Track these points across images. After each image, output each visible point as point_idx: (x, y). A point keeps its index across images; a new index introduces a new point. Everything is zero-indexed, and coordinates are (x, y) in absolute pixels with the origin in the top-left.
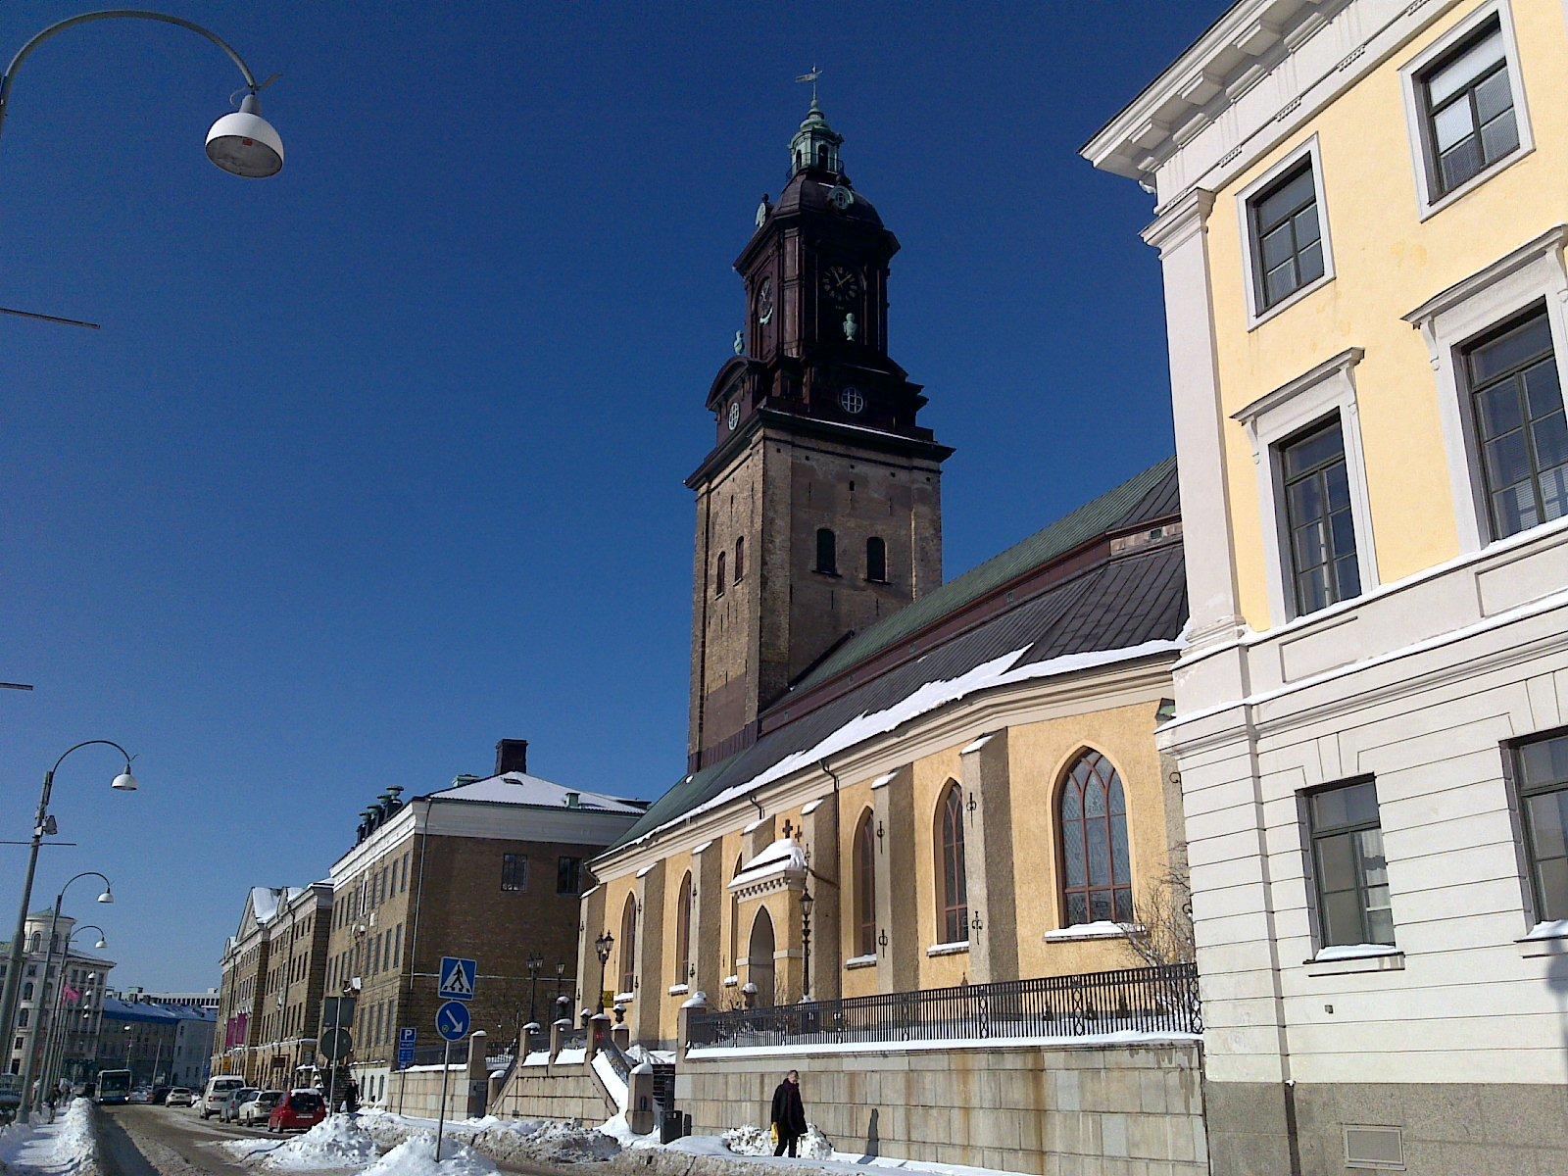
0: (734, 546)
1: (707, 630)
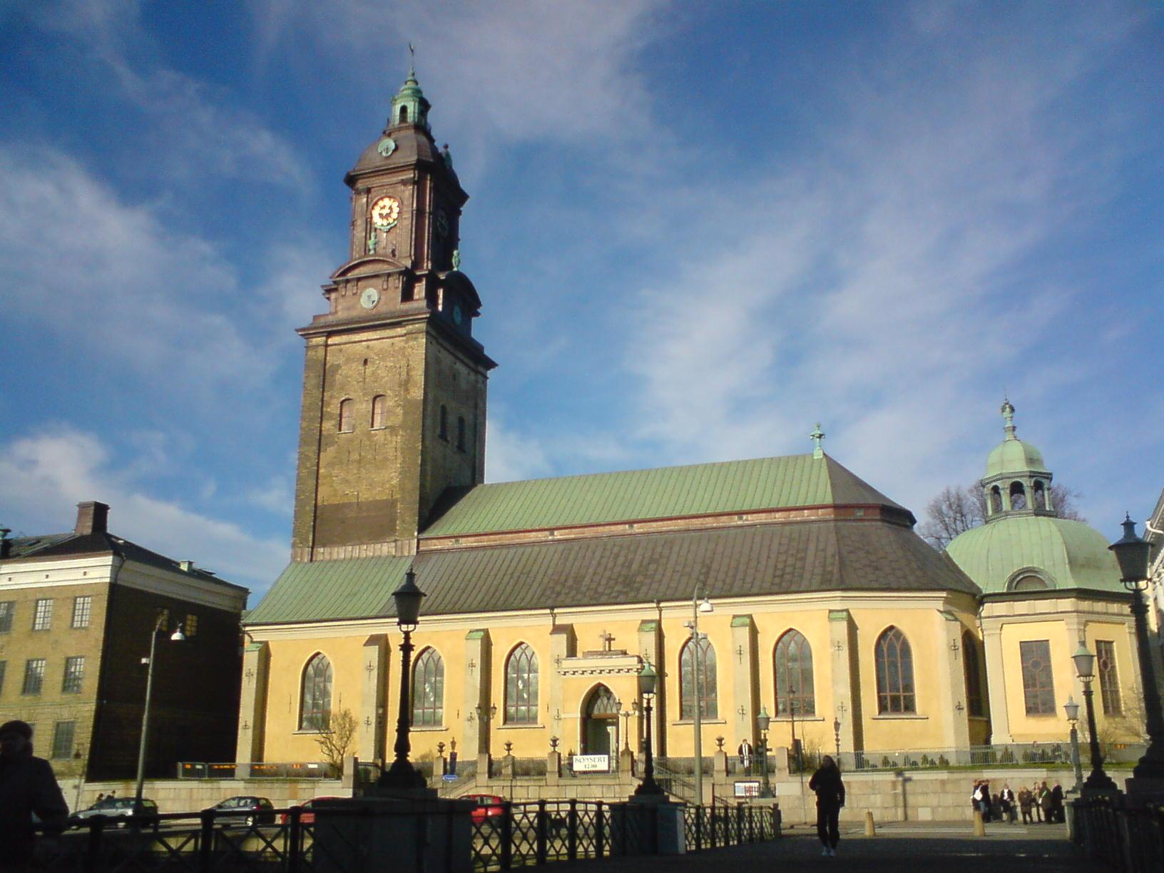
0: (370, 398)
1: (322, 454)
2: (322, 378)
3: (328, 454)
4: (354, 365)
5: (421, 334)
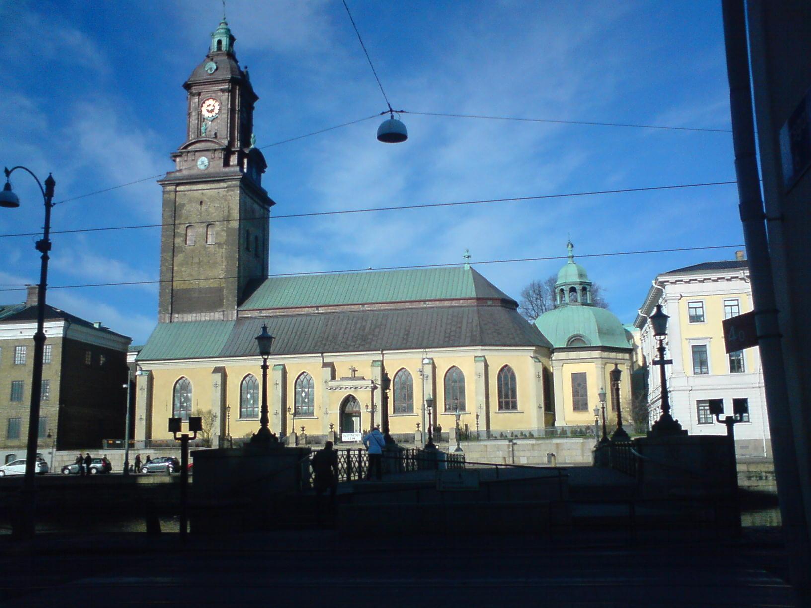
1: (175, 258)
2: (174, 212)
3: (179, 258)
4: (194, 205)
5: (236, 189)
